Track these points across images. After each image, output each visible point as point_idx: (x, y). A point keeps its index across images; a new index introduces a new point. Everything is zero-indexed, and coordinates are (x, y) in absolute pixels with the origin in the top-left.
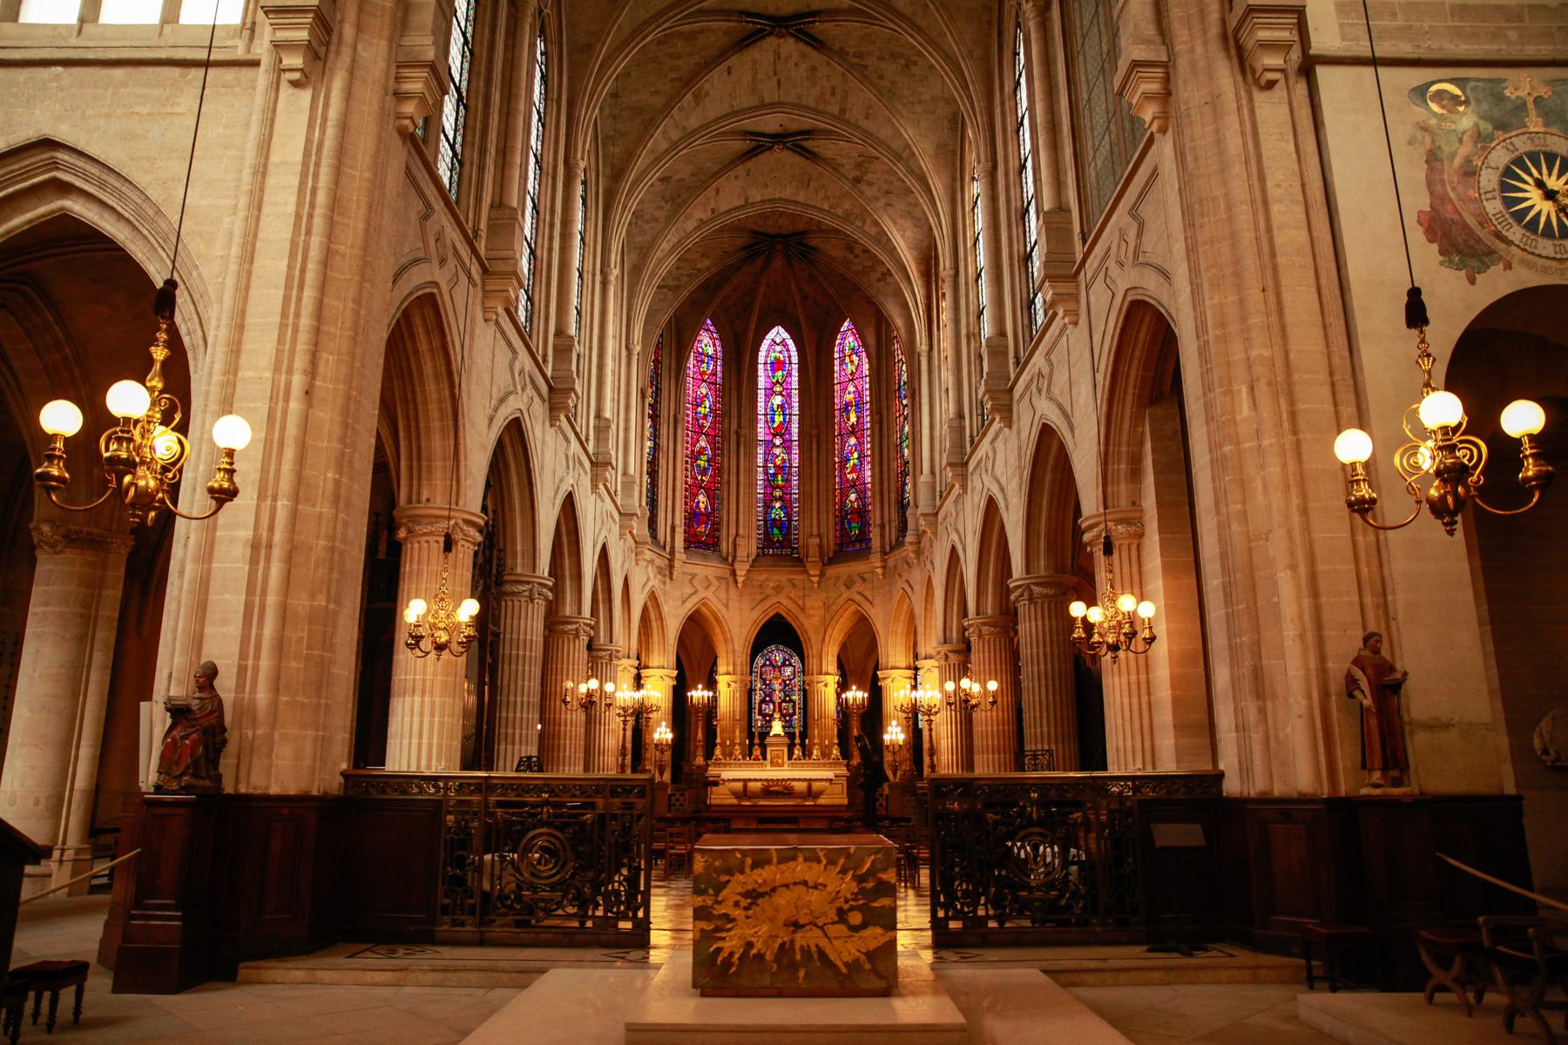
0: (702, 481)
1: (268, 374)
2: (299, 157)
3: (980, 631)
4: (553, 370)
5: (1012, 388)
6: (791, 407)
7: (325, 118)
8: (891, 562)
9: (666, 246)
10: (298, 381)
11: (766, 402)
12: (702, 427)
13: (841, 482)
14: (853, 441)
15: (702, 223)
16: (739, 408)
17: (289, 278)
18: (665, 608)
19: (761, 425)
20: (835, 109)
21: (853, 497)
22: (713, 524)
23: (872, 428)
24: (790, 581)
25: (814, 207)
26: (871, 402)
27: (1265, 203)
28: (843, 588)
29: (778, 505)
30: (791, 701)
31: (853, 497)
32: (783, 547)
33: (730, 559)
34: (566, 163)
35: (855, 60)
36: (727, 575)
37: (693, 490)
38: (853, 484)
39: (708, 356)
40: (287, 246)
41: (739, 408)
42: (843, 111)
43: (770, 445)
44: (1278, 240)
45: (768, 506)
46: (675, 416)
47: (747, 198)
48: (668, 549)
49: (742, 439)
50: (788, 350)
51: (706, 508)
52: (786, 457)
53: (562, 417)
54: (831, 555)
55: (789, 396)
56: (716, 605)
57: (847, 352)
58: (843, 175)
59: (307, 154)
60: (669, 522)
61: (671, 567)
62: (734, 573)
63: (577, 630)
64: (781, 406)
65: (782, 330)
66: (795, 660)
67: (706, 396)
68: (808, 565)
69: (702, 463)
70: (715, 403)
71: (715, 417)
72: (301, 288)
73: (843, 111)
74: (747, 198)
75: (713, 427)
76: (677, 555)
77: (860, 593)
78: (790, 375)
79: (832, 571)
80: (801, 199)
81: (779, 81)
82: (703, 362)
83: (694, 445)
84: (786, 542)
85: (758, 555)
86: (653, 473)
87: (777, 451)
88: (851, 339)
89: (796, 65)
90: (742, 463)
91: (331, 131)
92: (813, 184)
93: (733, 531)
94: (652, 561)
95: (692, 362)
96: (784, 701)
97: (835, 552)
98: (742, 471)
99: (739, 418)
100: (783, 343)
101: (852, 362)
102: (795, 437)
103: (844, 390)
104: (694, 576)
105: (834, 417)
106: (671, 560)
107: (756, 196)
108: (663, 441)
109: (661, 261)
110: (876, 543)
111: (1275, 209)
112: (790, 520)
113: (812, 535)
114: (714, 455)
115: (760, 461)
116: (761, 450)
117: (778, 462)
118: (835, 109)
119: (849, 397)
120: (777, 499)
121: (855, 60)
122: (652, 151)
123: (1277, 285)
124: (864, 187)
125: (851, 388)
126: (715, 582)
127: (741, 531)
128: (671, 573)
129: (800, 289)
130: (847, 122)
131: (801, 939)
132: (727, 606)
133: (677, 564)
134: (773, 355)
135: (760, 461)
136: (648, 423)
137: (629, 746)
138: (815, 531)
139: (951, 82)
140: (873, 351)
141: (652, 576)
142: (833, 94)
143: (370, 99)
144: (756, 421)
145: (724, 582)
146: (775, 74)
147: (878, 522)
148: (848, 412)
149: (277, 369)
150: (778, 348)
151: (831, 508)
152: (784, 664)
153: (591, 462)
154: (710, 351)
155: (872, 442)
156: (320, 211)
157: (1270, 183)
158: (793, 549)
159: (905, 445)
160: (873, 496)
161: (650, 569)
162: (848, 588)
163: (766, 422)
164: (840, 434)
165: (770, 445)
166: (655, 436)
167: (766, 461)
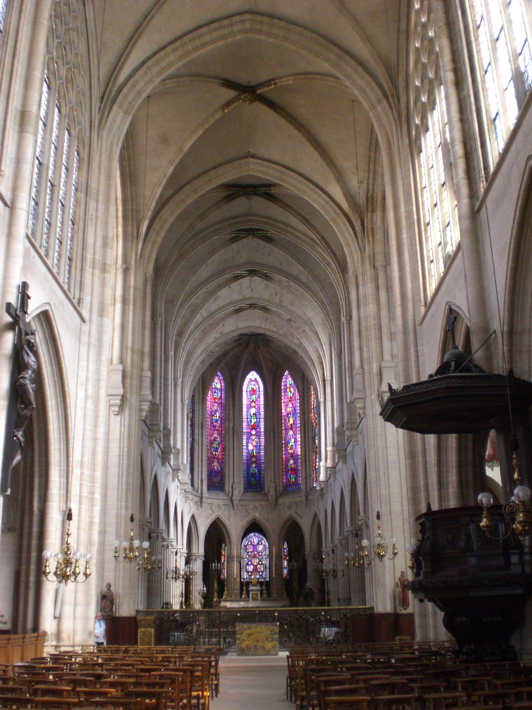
0: (216, 455)
1: (115, 503)
2: (118, 437)
3: (341, 542)
4: (163, 444)
5: (346, 449)
6: (260, 414)
7: (124, 425)
8: (310, 497)
9: (199, 351)
10: (123, 504)
11: (247, 412)
12: (215, 427)
13: (286, 454)
15: (216, 339)
16: (234, 414)
17: (119, 474)
18: (199, 522)
19: (245, 424)
20: (277, 301)
21: (292, 462)
22: (221, 477)
23: (301, 427)
24: (261, 505)
25: (270, 330)
26: (300, 413)
27: (386, 449)
29: (254, 465)
30: (262, 564)
31: (292, 462)
32: (256, 488)
33: (230, 495)
35: (285, 284)
36: (229, 503)
37: (211, 459)
39: (217, 389)
40: (117, 464)
41: (234, 414)
43: (249, 435)
44: (389, 459)
46: (202, 423)
47: (237, 327)
48: (199, 492)
49: (235, 432)
50: (258, 384)
52: (257, 440)
54: (281, 492)
55: (259, 408)
56: (224, 519)
58: (282, 318)
59: (120, 436)
60: (200, 478)
62: (232, 501)
63: (168, 544)
64: (255, 414)
66: (265, 542)
67: (216, 410)
68: (270, 498)
69: (215, 445)
70: (221, 413)
71: (221, 421)
72: (122, 477)
73: (281, 302)
74: (237, 327)
75: (221, 426)
76: (204, 495)
77: (295, 512)
78: (259, 397)
79: (281, 501)
80: (263, 326)
81: (252, 289)
82: (215, 392)
83: (211, 436)
85: (244, 492)
88: (290, 379)
89: (259, 283)
90: (235, 445)
91: (126, 429)
92: (269, 321)
93: (231, 481)
94: (192, 499)
95: (210, 393)
96: (259, 564)
97: (283, 490)
98: (235, 449)
99: (234, 421)
100: (256, 380)
101: (290, 391)
102: (262, 430)
103: (287, 406)
104: (212, 504)
105: (282, 420)
106: (201, 498)
107: (242, 325)
108: (196, 437)
109: (197, 358)
110: (303, 487)
111: (389, 450)
112: (260, 473)
113: (271, 482)
114: (221, 441)
118: (277, 301)
120: (253, 462)
121: (285, 284)
122: (196, 322)
123: (388, 473)
124: (292, 323)
125: (290, 405)
126: (222, 507)
127: (235, 481)
129: (264, 356)
130: (283, 307)
131: (259, 644)
132: (229, 519)
133: (204, 500)
134: (251, 387)
135: (244, 442)
137: (184, 592)
138: (273, 481)
140: (301, 388)
141: (192, 507)
142: (276, 294)
143: (134, 413)
144: (241, 421)
145: (227, 507)
146: (250, 286)
147: (304, 476)
148: (289, 418)
149: (118, 501)
150: (253, 383)
151: (281, 467)
152: (258, 544)
153: (172, 469)
154: (219, 386)
155: (301, 434)
156: (125, 454)
157: (388, 442)
158: (261, 488)
159: (317, 437)
160: (301, 462)
161: (192, 504)
162: (290, 510)
163: (248, 422)
164: (285, 429)
165: (249, 435)
166: (193, 434)
167: (248, 443)
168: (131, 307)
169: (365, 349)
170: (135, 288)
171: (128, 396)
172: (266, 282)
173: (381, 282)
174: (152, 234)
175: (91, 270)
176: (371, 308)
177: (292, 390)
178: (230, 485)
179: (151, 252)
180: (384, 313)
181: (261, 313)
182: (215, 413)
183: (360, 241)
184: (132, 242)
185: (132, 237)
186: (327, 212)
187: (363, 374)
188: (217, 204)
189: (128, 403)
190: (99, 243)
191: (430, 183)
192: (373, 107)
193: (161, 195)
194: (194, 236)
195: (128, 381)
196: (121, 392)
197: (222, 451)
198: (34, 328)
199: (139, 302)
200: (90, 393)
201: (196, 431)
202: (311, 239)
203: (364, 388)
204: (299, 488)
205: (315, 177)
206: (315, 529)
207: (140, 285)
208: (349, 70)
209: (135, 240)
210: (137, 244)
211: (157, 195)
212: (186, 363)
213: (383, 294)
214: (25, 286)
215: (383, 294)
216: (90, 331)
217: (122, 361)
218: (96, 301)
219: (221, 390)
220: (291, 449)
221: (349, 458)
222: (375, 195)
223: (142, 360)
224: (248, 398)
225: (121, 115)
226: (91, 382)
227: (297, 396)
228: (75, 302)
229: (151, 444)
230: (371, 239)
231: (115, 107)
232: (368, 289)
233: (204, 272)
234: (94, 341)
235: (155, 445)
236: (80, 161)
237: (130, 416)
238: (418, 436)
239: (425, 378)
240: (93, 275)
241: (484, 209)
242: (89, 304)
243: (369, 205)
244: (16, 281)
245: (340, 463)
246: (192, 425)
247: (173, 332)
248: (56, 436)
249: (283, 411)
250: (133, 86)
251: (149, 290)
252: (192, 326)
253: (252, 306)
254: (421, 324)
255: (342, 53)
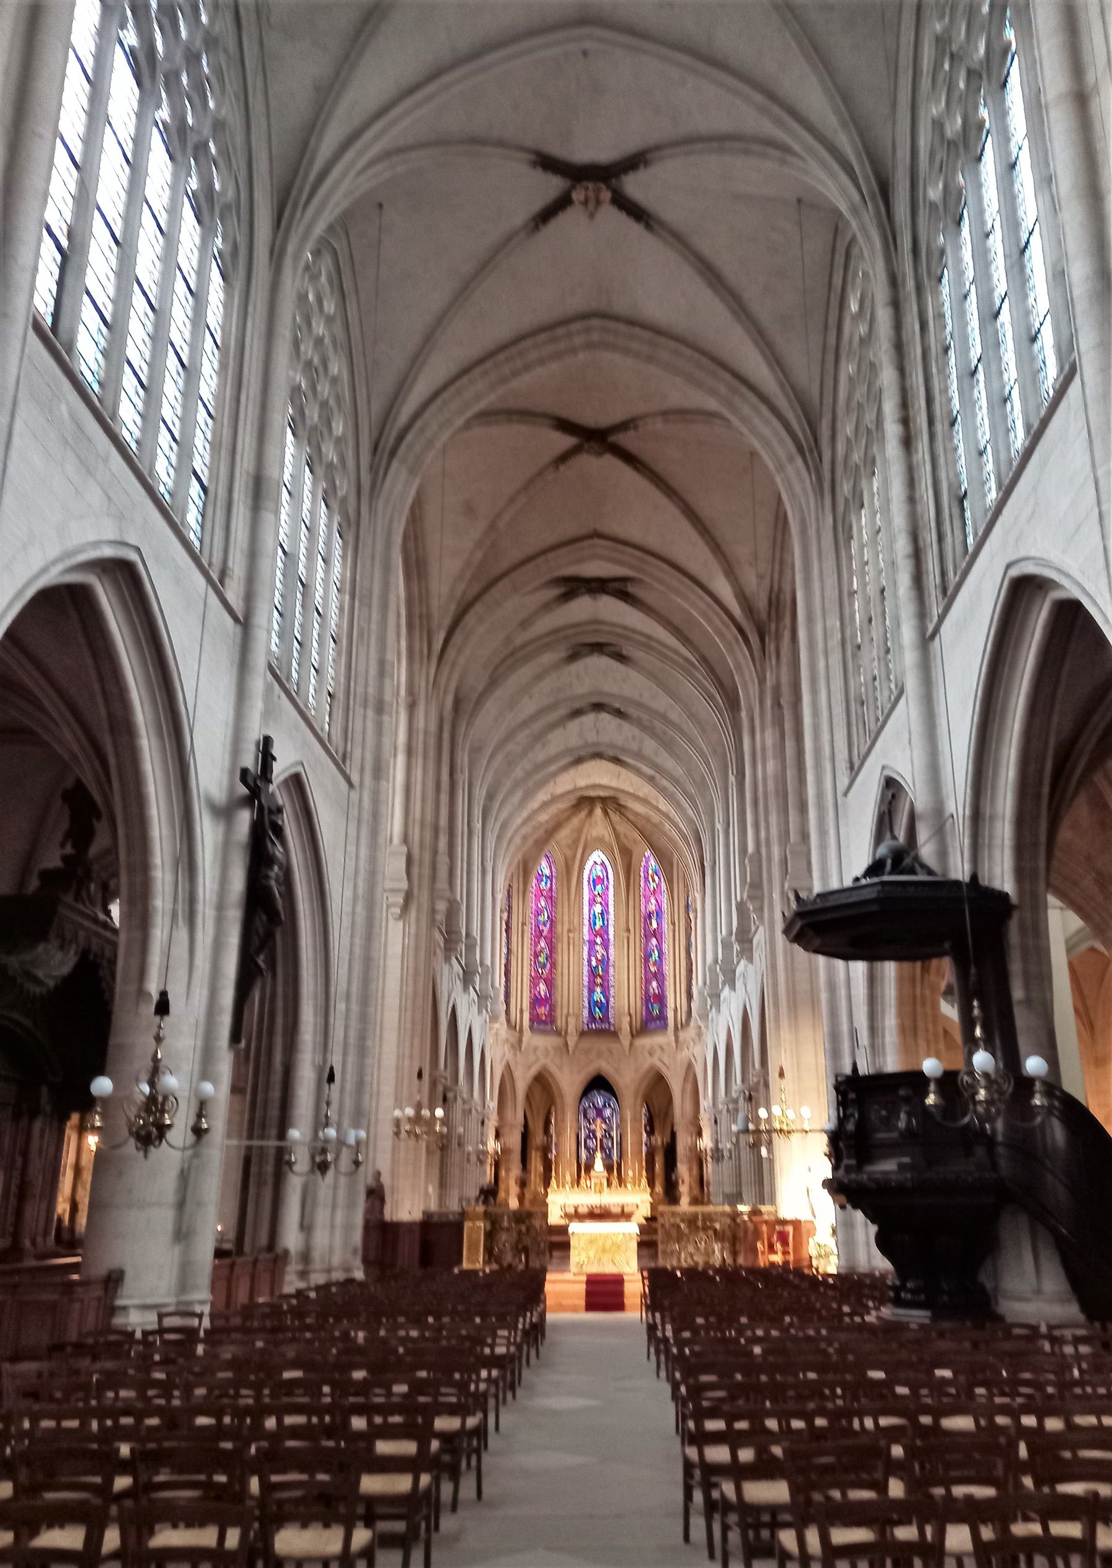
1: (395, 1049)
2: (400, 952)
6: (608, 912)
8: (681, 1038)
10: (407, 1051)
12: (541, 932)
14: (654, 941)
21: (654, 984)
22: (551, 1006)
28: (647, 1054)
31: (654, 984)
34: (469, 825)
37: (534, 982)
38: (655, 975)
42: (640, 750)
43: (592, 944)
45: (591, 991)
51: (545, 995)
53: (471, 988)
56: (554, 1069)
57: (650, 872)
59: (403, 949)
60: (519, 1007)
61: (520, 1041)
62: (566, 1044)
64: (602, 914)
65: (601, 853)
78: (607, 888)
83: (536, 946)
84: (605, 1019)
86: (507, 973)
87: (598, 948)
91: (412, 941)
93: (565, 1011)
100: (603, 864)
101: (654, 880)
115: (586, 957)
116: (586, 949)
117: (599, 957)
119: (652, 907)
125: (653, 901)
126: (552, 1052)
127: (571, 1011)
128: (520, 1047)
129: (614, 829)
133: (525, 1039)
136: (504, 934)
139: (703, 768)
147: (673, 1006)
148: (650, 918)
149: (398, 1046)
154: (547, 872)
167: (590, 955)
168: (420, 761)
169: (762, 824)
170: (426, 733)
171: (416, 891)
172: (618, 721)
173: (788, 726)
174: (451, 652)
175: (362, 710)
176: (771, 766)
177: (656, 878)
178: (564, 1020)
179: (449, 679)
180: (790, 773)
181: (611, 766)
182: (542, 912)
183: (758, 664)
184: (421, 663)
185: (421, 657)
186: (710, 621)
187: (760, 860)
188: (547, 607)
189: (415, 902)
190: (373, 671)
191: (864, 585)
192: (781, 468)
193: (464, 592)
194: (512, 654)
195: (415, 870)
196: (404, 885)
197: (551, 970)
198: (280, 802)
199: (432, 753)
200: (361, 891)
201: (514, 938)
202: (687, 660)
203: (761, 881)
204: (665, 1026)
205: (694, 568)
206: (689, 1087)
207: (433, 728)
208: (746, 410)
209: (425, 661)
210: (428, 666)
211: (459, 594)
212: (499, 838)
213: (790, 745)
214: (267, 741)
215: (790, 745)
216: (360, 800)
217: (406, 839)
218: (369, 756)
219: (550, 878)
220: (655, 964)
221: (739, 984)
222: (782, 597)
223: (436, 837)
224: (590, 890)
225: (404, 475)
226: (362, 874)
227: (663, 886)
228: (339, 759)
229: (447, 959)
230: (774, 662)
231: (395, 464)
232: (770, 737)
233: (528, 707)
234: (366, 816)
235: (454, 960)
236: (344, 548)
237: (418, 920)
238: (840, 964)
239: (848, 883)
240: (365, 717)
241: (937, 639)
242: (360, 761)
243: (773, 612)
244: (254, 733)
245: (727, 988)
246: (508, 930)
247: (480, 794)
248: (311, 955)
249: (643, 909)
250: (422, 430)
251: (446, 736)
252: (508, 784)
253: (598, 755)
254: (846, 794)
255: (736, 383)
